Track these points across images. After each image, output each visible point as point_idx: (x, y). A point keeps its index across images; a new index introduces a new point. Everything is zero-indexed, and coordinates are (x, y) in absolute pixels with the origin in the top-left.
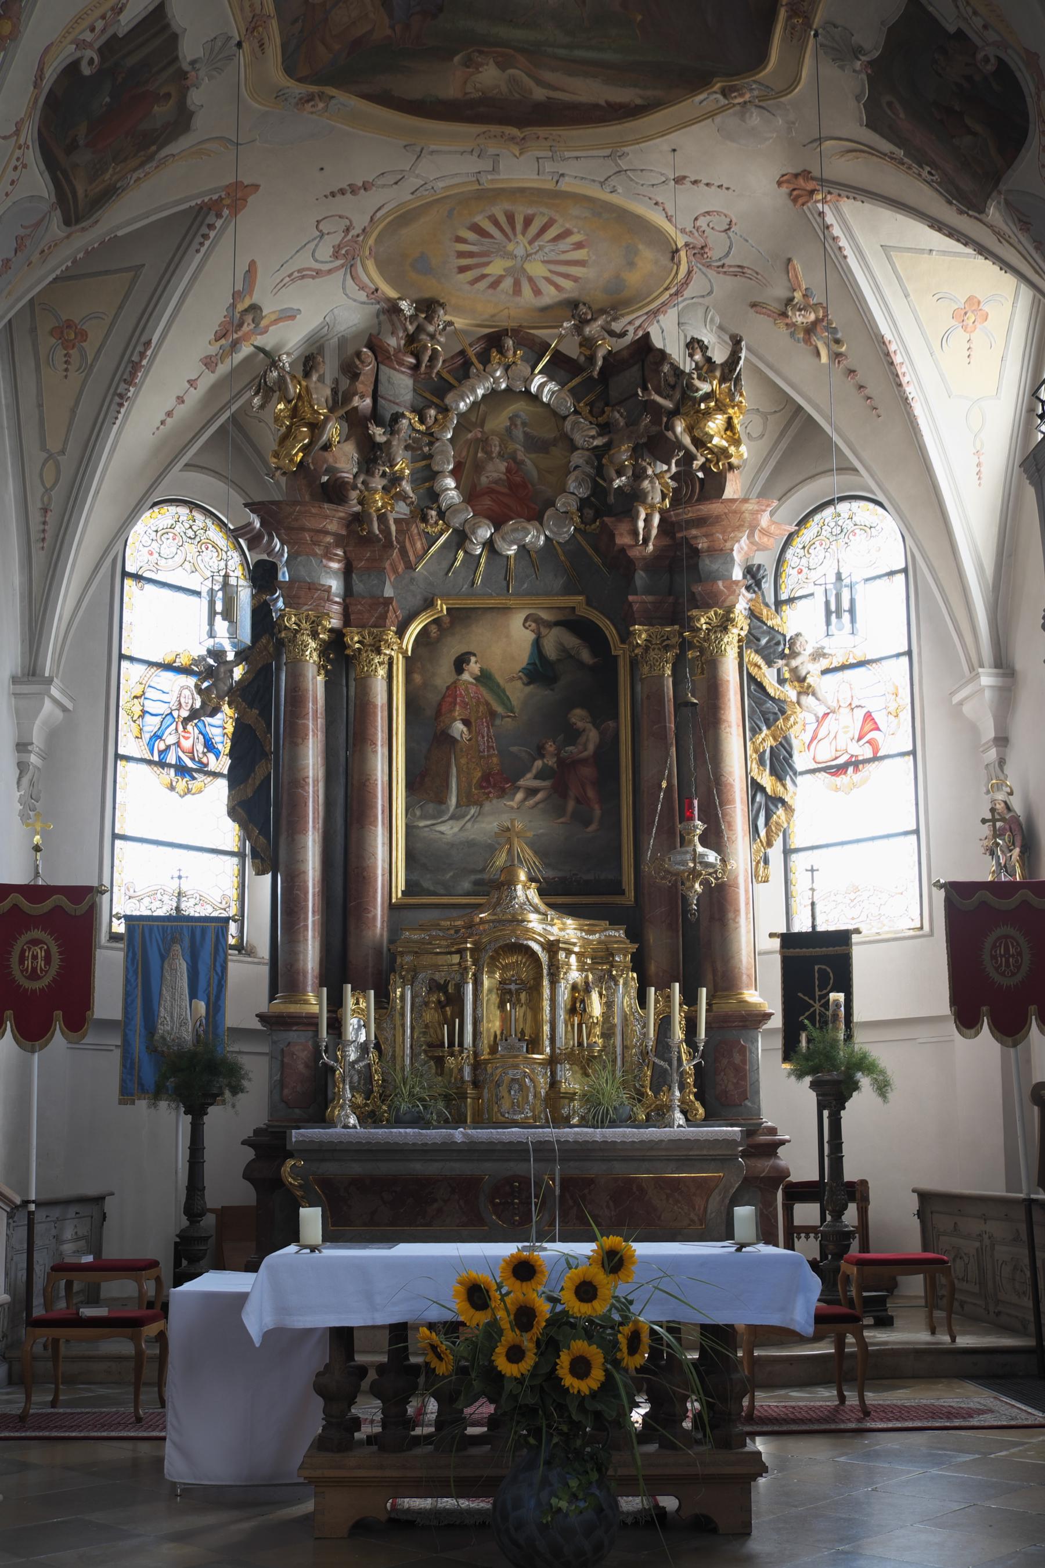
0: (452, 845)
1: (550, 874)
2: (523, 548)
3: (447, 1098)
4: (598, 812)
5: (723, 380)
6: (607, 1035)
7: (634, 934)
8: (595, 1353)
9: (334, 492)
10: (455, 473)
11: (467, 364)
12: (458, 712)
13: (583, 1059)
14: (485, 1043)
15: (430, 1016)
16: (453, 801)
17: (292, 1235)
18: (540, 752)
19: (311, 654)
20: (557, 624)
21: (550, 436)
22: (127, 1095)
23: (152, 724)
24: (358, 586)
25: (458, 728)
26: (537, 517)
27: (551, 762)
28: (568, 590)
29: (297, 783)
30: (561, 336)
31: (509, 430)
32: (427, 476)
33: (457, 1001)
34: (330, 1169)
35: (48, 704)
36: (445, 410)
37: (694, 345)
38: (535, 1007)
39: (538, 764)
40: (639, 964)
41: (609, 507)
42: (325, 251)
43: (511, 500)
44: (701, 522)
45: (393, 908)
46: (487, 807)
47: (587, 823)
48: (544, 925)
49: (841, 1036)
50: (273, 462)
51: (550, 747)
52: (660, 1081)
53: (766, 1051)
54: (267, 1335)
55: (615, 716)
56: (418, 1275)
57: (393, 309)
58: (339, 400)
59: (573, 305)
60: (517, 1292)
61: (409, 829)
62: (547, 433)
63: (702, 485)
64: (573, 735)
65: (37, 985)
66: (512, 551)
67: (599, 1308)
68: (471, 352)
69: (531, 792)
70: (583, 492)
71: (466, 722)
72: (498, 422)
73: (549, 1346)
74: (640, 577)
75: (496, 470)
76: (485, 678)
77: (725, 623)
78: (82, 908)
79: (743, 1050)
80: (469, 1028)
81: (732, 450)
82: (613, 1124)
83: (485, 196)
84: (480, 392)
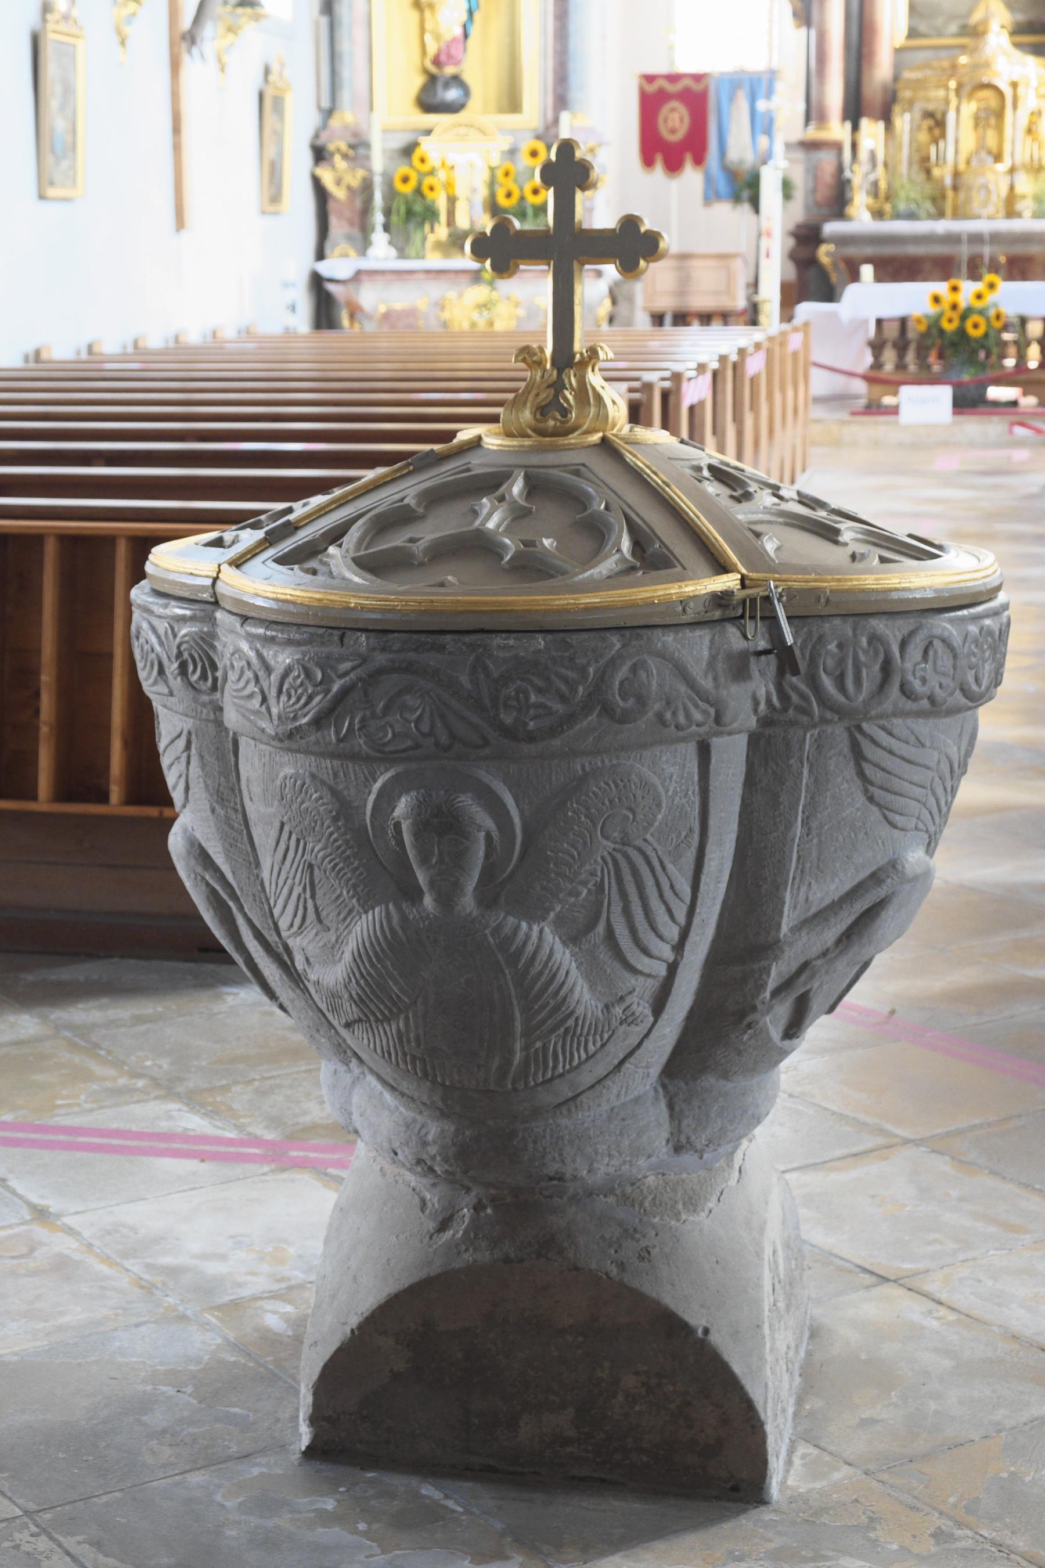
1: (1021, 17)
3: (934, 200)
15: (923, 137)
38: (1000, 129)
56: (913, 299)
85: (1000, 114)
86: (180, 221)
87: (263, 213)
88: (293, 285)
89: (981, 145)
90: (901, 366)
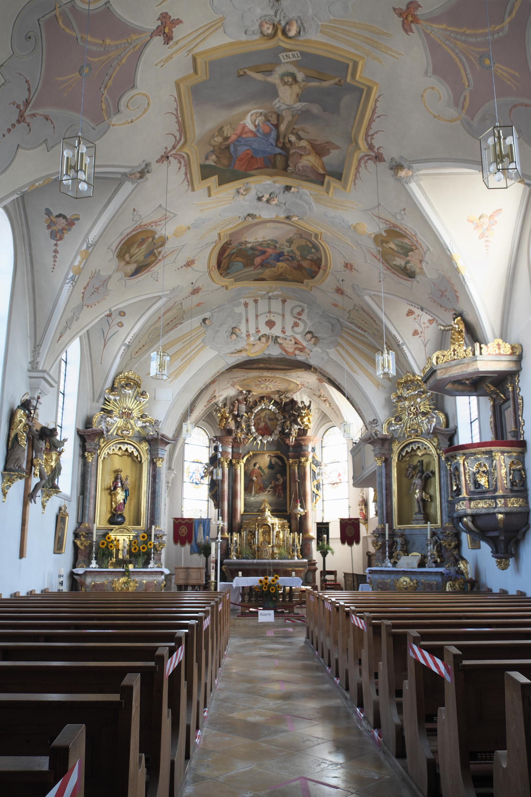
0: (253, 502)
1: (273, 508)
2: (268, 442)
3: (252, 554)
4: (282, 495)
5: (308, 409)
6: (283, 541)
7: (289, 521)
8: (274, 588)
9: (229, 432)
10: (254, 425)
11: (256, 403)
12: (254, 475)
13: (279, 546)
14: (260, 543)
15: (249, 537)
16: (253, 493)
17: (238, 576)
18: (271, 483)
19: (226, 465)
20: (275, 457)
21: (273, 418)
22: (191, 553)
23: (191, 474)
24: (235, 451)
25: (254, 478)
26: (270, 435)
27: (273, 485)
28: (277, 450)
29: (223, 492)
30: (276, 397)
31: (265, 416)
32: (248, 426)
33: (254, 534)
34: (231, 567)
35: (173, 474)
36: (252, 412)
37: (302, 402)
38: (269, 536)
39: (270, 486)
40: (290, 527)
41: (285, 435)
42: (229, 385)
43: (265, 431)
44: (303, 440)
45: (241, 515)
46: (260, 494)
47: (280, 497)
48: (272, 520)
49: (326, 543)
50: (218, 427)
51: (273, 482)
52: (293, 551)
53: (314, 544)
54: (236, 587)
55: (286, 476)
56: (253, 581)
57: (241, 392)
58: (231, 412)
59: (278, 391)
60: (265, 581)
61: (245, 499)
62: (273, 417)
63: (303, 432)
64: (277, 480)
65: (184, 535)
66: (265, 442)
67: (274, 583)
68: (257, 400)
69: (269, 491)
70: (280, 429)
71: (256, 477)
72: (263, 414)
73: (269, 587)
74: (291, 449)
75: (262, 425)
76: (260, 468)
77: (307, 460)
78: (191, 522)
79: (309, 545)
80: (257, 540)
81: (309, 425)
82: (284, 559)
83: (260, 377)
84: (259, 408)
85: (269, 532)
86: (22, 555)
87: (54, 553)
88: (63, 576)
89: (264, 539)
90: (250, 601)
